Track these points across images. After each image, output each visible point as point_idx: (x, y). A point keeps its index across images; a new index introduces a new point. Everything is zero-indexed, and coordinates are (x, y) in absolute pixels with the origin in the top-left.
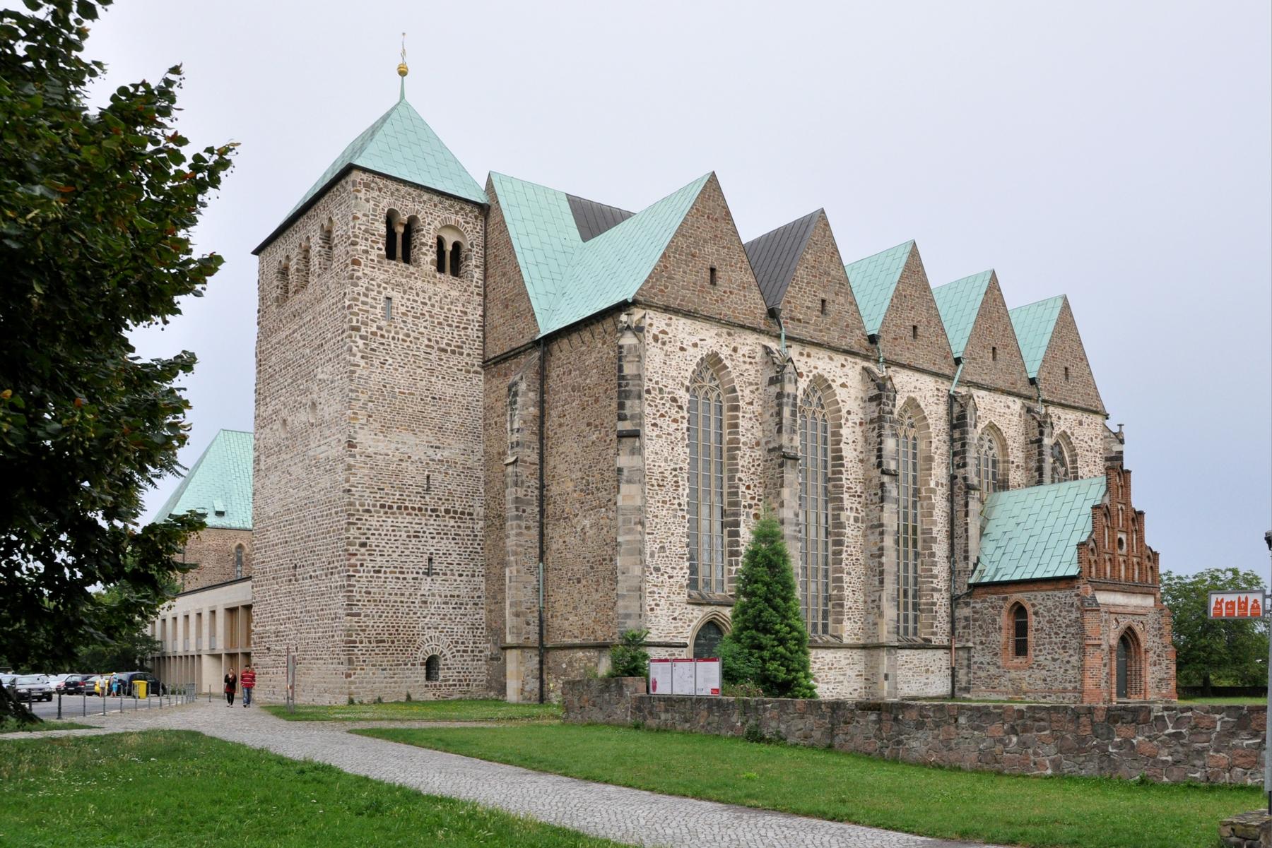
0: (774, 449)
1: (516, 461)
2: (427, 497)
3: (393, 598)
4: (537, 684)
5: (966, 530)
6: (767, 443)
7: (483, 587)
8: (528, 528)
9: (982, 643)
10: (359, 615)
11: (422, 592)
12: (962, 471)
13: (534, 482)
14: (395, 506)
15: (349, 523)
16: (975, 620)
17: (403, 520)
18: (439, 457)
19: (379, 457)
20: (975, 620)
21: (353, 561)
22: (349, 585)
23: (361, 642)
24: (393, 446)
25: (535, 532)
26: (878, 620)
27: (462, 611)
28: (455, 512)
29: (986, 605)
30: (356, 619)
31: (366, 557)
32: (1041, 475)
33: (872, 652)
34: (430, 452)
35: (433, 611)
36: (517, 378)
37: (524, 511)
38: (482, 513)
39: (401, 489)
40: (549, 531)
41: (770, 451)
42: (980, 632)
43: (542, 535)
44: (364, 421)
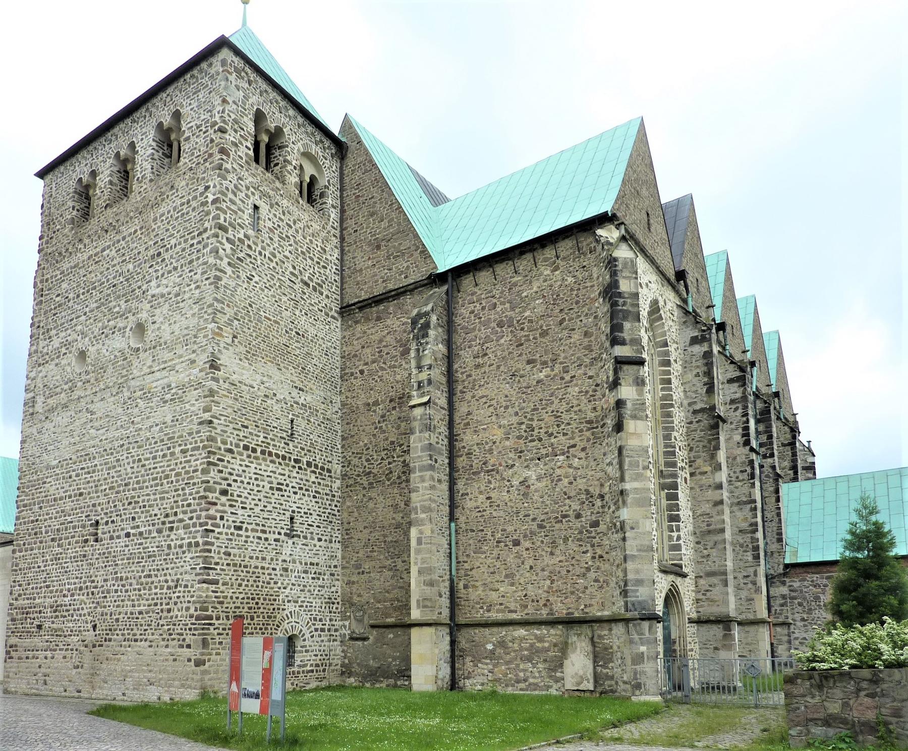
0: (702, 410)
1: (429, 401)
2: (291, 444)
3: (254, 563)
4: (448, 670)
5: (779, 515)
6: (690, 404)
7: (339, 555)
8: (439, 481)
9: (803, 620)
10: (216, 582)
11: (283, 557)
12: (769, 460)
13: (443, 429)
14: (259, 449)
15: (209, 463)
16: (793, 598)
17: (267, 467)
18: (301, 401)
19: (244, 387)
20: (793, 598)
21: (212, 512)
22: (206, 543)
23: (218, 619)
24: (259, 378)
25: (445, 486)
26: (754, 596)
27: (320, 582)
28: (316, 466)
29: (806, 583)
30: (213, 587)
31: (227, 508)
32: (796, 473)
33: (747, 628)
34: (295, 393)
35: (293, 580)
36: (429, 308)
37: (436, 461)
38: (339, 472)
39: (265, 431)
40: (460, 485)
41: (695, 412)
42: (800, 609)
43: (451, 490)
44: (229, 341)
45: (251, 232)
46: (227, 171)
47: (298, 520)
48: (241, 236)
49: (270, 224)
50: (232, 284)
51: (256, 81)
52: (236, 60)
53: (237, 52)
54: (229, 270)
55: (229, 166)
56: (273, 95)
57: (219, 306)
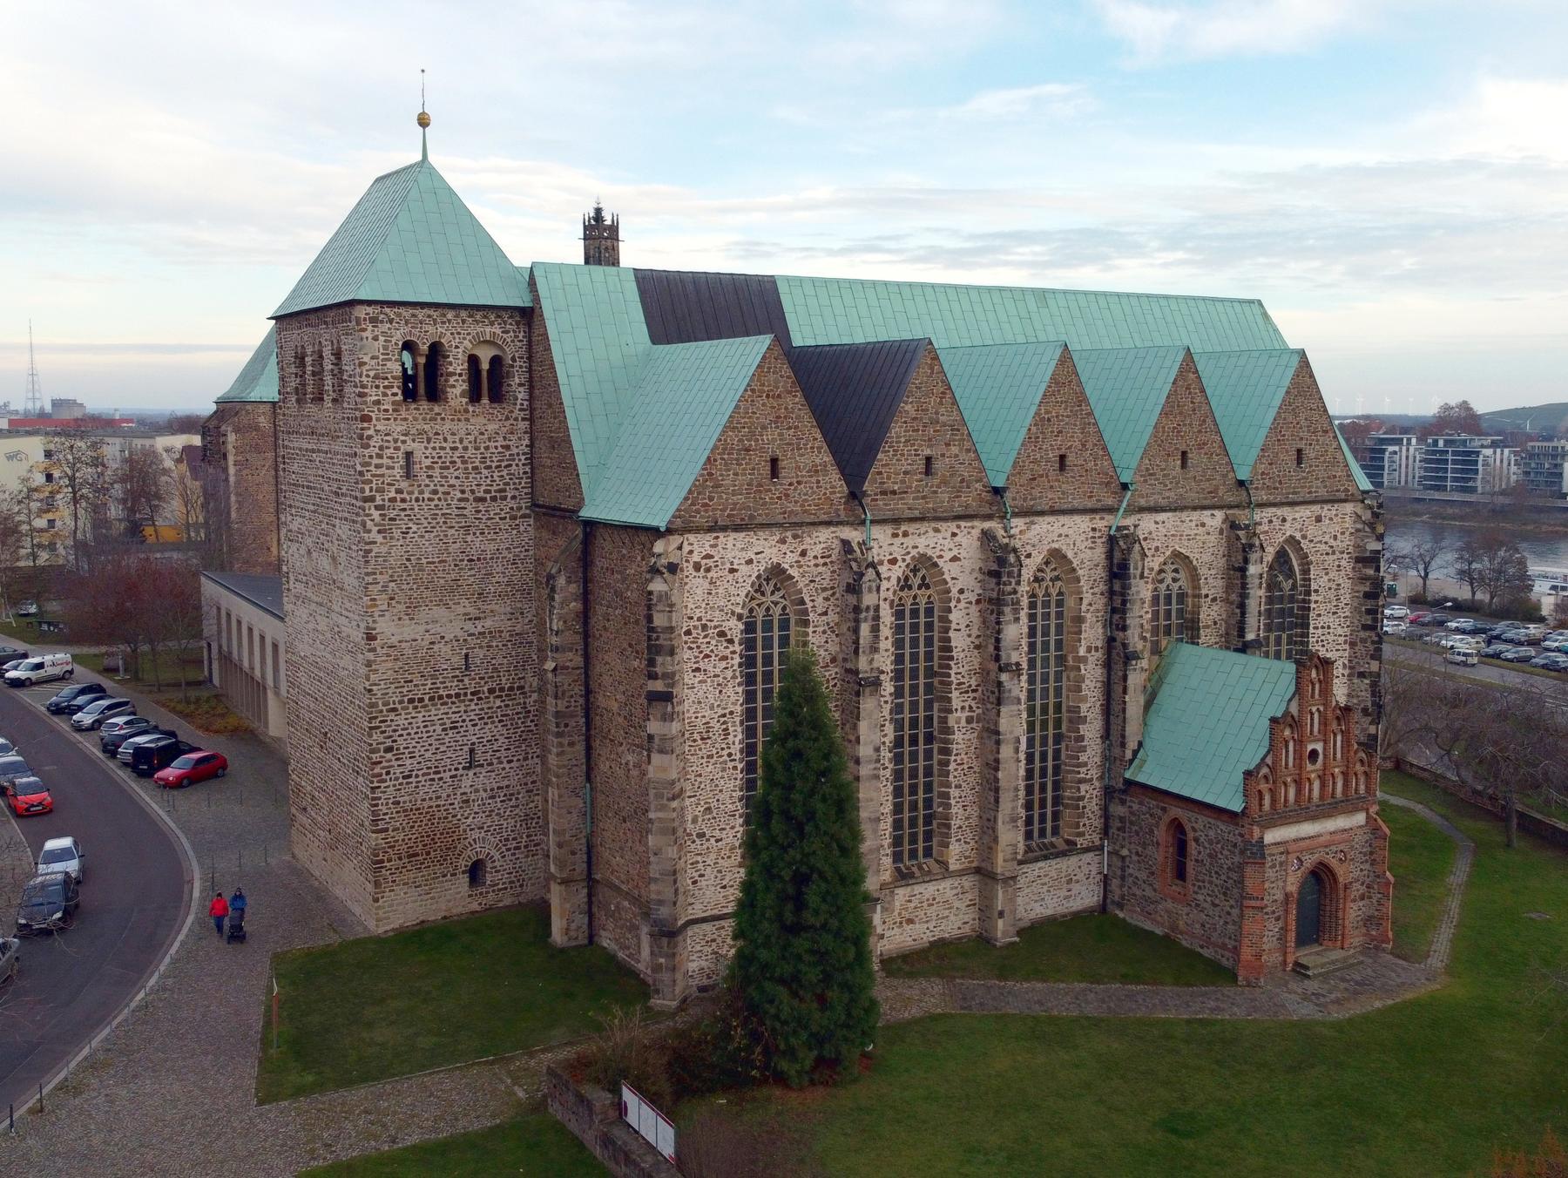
2: (466, 680)
3: (426, 804)
10: (386, 830)
18: (480, 629)
20: (1132, 823)
21: (377, 770)
23: (390, 860)
24: (422, 628)
30: (383, 835)
34: (469, 626)
44: (385, 607)
45: (404, 485)
46: (369, 437)
47: (479, 750)
48: (392, 494)
49: (428, 462)
50: (384, 549)
51: (399, 315)
52: (370, 310)
53: (369, 303)
54: (379, 538)
55: (371, 432)
56: (421, 313)
57: (370, 579)
